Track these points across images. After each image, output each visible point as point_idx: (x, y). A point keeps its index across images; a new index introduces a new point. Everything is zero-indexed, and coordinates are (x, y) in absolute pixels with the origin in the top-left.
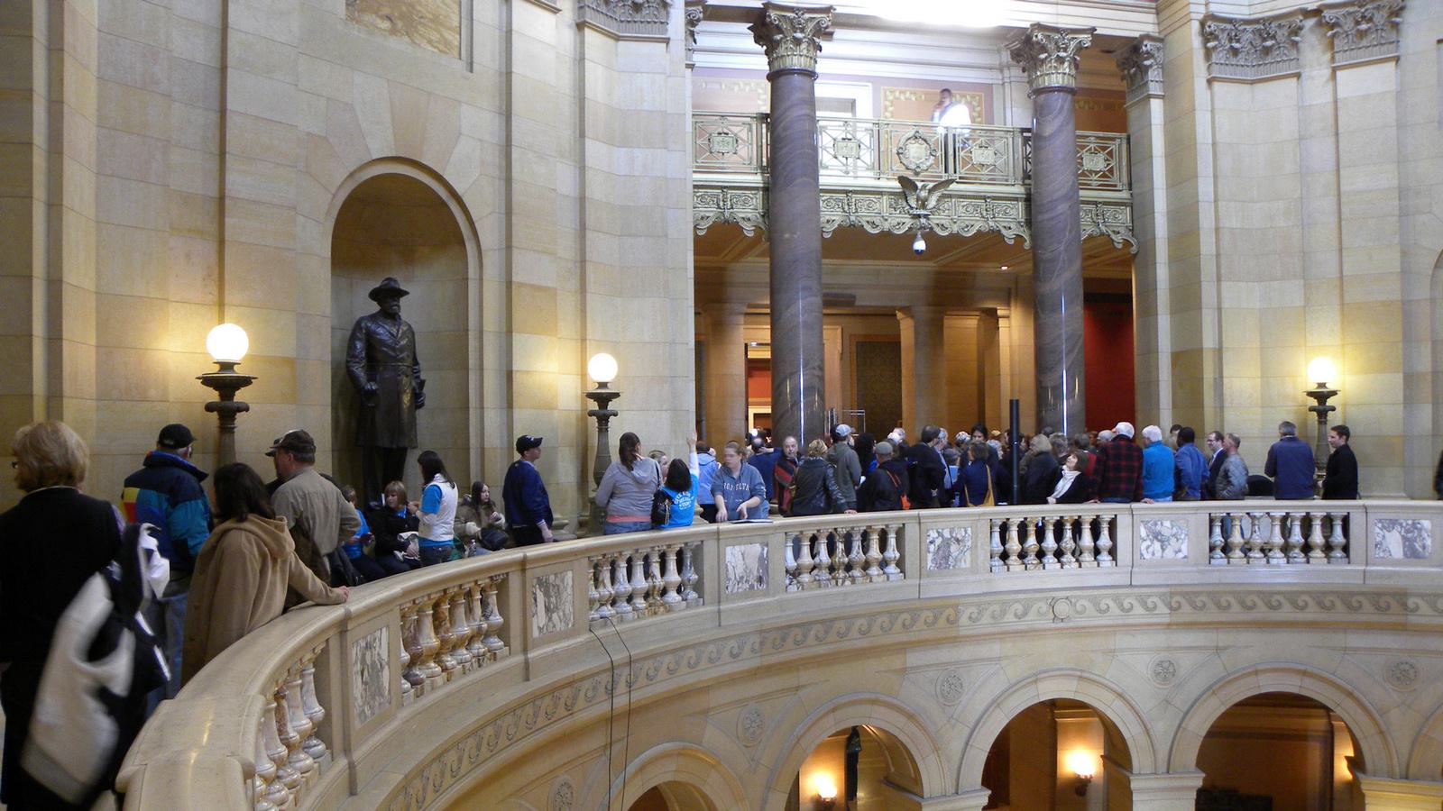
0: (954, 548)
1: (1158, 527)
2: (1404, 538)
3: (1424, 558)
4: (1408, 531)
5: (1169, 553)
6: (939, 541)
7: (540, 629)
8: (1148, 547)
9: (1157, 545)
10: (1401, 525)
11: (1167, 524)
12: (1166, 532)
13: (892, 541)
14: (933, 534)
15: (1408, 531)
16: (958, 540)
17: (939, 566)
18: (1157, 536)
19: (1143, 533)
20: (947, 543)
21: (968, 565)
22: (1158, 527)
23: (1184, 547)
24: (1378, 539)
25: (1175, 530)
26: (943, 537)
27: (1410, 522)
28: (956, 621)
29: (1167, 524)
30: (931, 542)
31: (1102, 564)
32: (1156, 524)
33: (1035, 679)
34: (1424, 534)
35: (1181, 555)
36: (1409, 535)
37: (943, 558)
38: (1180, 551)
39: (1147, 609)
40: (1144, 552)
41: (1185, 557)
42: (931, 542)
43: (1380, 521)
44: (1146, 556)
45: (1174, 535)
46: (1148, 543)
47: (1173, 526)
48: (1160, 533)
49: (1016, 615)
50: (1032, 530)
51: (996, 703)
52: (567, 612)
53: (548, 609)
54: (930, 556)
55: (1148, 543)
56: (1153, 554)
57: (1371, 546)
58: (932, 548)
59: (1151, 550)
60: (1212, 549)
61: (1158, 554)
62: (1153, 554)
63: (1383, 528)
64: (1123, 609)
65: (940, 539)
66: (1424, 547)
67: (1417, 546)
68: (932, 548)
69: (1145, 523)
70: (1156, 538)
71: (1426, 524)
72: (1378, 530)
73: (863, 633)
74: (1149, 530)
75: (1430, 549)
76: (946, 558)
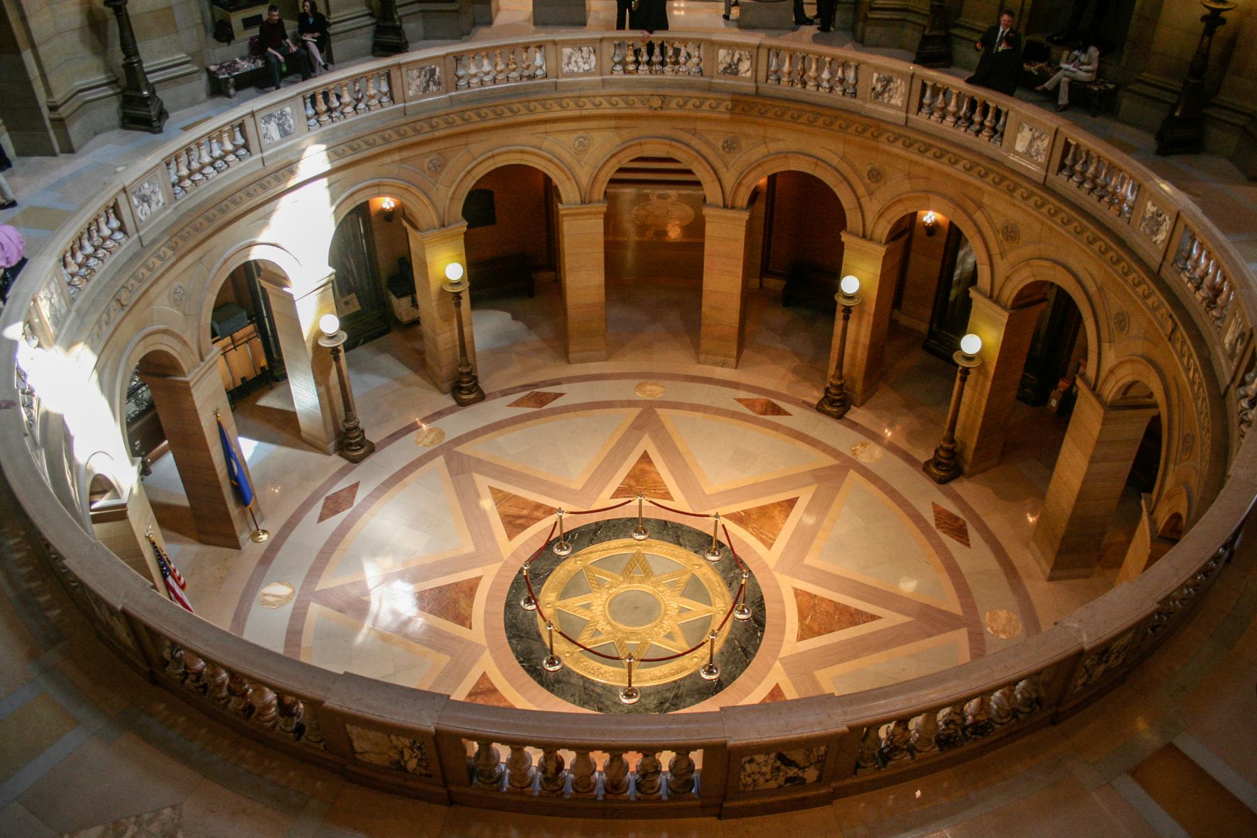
1: (143, 192)
2: (279, 125)
3: (291, 134)
4: (279, 119)
10: (274, 116)
11: (146, 185)
12: (147, 192)
15: (279, 119)
19: (135, 201)
22: (143, 192)
24: (264, 132)
27: (279, 112)
29: (146, 185)
32: (140, 190)
34: (288, 117)
36: (281, 122)
43: (263, 118)
48: (145, 196)
57: (261, 137)
63: (266, 122)
66: (290, 126)
67: (286, 127)
70: (143, 201)
71: (288, 110)
72: (263, 126)
75: (293, 127)
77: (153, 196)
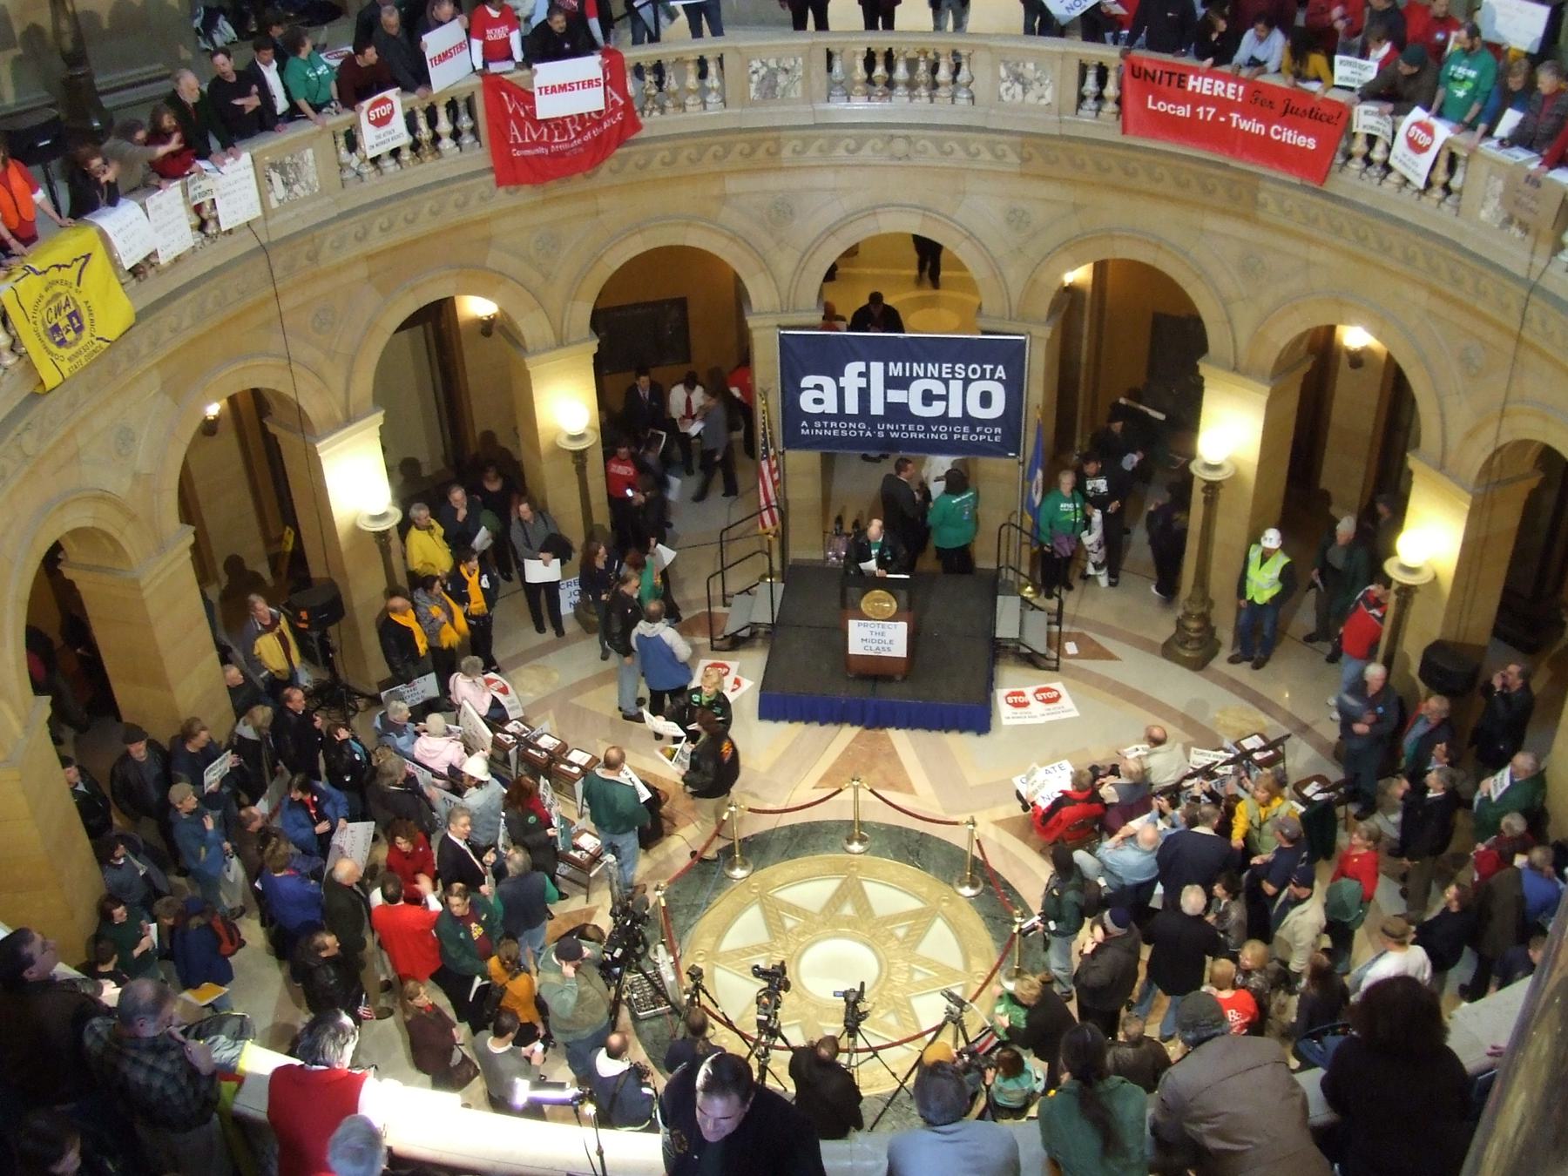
0: (782, 79)
1: (1020, 69)
5: (1031, 97)
6: (763, 71)
7: (280, 201)
8: (1008, 89)
9: (1018, 88)
13: (712, 69)
14: (756, 64)
16: (786, 71)
17: (765, 96)
18: (1018, 78)
19: (1003, 73)
20: (772, 73)
21: (799, 94)
23: (1049, 94)
25: (1038, 74)
26: (767, 66)
28: (778, 151)
29: (1031, 66)
30: (754, 72)
31: (958, 101)
32: (1018, 65)
33: (873, 211)
35: (1044, 102)
37: (769, 86)
38: (1042, 97)
39: (996, 156)
40: (1004, 94)
41: (1049, 104)
42: (754, 72)
44: (1006, 98)
45: (1038, 80)
46: (1008, 84)
47: (1036, 70)
49: (848, 150)
50: (880, 60)
51: (831, 232)
52: (310, 181)
53: (286, 184)
54: (753, 86)
55: (1008, 84)
56: (1013, 97)
58: (755, 78)
59: (1011, 91)
60: (1082, 98)
61: (1019, 97)
62: (1013, 97)
64: (969, 154)
65: (765, 69)
68: (755, 78)
69: (1006, 63)
73: (641, 167)
74: (1010, 70)
76: (773, 87)
77: (1036, 85)
